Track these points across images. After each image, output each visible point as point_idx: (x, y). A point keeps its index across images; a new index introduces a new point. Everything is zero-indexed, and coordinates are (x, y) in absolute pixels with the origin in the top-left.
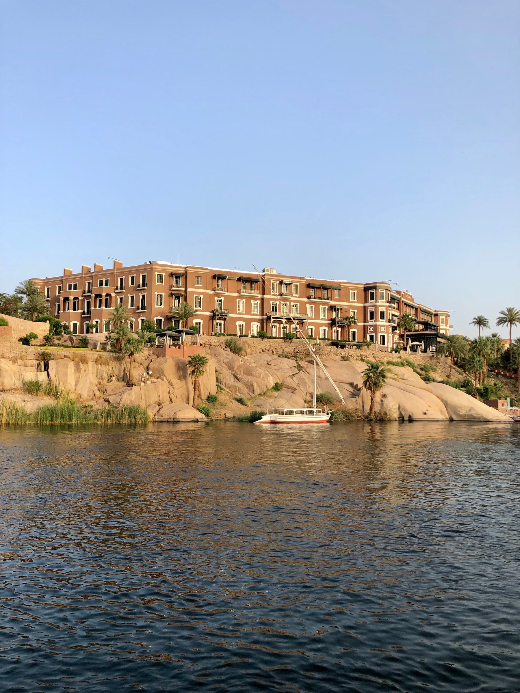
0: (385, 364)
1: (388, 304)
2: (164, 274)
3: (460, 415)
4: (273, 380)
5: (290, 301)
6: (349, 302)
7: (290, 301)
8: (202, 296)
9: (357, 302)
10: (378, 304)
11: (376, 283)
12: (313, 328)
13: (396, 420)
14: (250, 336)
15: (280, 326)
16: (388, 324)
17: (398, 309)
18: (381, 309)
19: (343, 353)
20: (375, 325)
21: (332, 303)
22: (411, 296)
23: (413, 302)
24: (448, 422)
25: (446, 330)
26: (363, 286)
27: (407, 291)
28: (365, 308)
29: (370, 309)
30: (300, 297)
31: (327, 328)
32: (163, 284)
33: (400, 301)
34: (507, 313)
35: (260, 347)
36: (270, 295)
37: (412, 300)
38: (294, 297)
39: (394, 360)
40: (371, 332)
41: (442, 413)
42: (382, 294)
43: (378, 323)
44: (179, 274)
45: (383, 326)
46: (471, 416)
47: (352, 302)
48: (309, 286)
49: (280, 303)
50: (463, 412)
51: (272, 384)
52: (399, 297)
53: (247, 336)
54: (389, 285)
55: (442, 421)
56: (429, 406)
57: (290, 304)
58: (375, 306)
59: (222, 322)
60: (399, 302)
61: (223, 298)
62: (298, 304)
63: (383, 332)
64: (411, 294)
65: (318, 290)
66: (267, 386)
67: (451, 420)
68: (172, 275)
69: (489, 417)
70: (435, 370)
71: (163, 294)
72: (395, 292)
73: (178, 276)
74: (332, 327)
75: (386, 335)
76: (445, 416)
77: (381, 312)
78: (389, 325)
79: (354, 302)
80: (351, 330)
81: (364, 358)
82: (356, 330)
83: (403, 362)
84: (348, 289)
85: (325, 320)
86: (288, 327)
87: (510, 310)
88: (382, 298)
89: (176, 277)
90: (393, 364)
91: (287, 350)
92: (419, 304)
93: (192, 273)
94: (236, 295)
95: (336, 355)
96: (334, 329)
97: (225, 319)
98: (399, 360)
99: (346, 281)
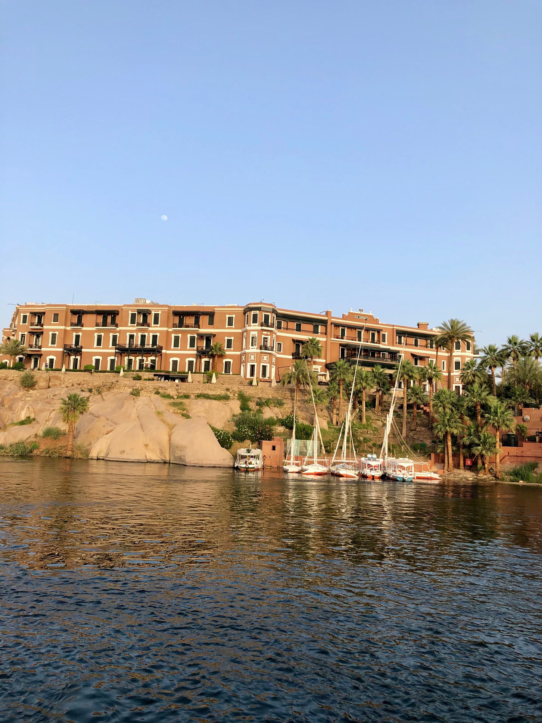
0: (192, 396)
1: (260, 328)
2: (28, 314)
3: (175, 457)
4: (25, 414)
5: (149, 332)
6: (225, 328)
7: (149, 332)
8: (57, 333)
9: (235, 328)
10: (248, 328)
11: (249, 304)
12: (178, 359)
13: (92, 459)
14: (64, 370)
15: (135, 359)
16: (259, 351)
17: (326, 334)
18: (252, 333)
19: (138, 385)
20: (245, 353)
21: (202, 331)
22: (372, 317)
23: (378, 324)
24: (168, 464)
25: (462, 357)
26: (243, 309)
27: (361, 310)
28: (243, 333)
29: (245, 334)
30: (160, 327)
31: (194, 360)
32: (27, 324)
33: (327, 323)
34: (450, 328)
35: (71, 381)
36: (128, 326)
37: (376, 321)
38: (154, 327)
39: (211, 393)
40: (252, 361)
41: (162, 452)
42: (255, 316)
43: (247, 351)
44: (40, 313)
45: (253, 353)
46: (180, 458)
47: (228, 328)
48: (176, 313)
49: (137, 334)
50: (178, 453)
51: (23, 417)
52: (326, 318)
53: (61, 370)
54: (271, 305)
55: (132, 462)
56: (146, 446)
57: (149, 334)
58: (246, 331)
59: (79, 358)
60: (324, 323)
61: (80, 334)
62: (158, 334)
63: (252, 361)
64: (371, 314)
65: (188, 318)
66: (12, 420)
67: (170, 463)
68: (34, 314)
69: (190, 459)
70: (280, 404)
71: (26, 333)
72: (324, 314)
73: (40, 315)
74: (201, 358)
75: (255, 364)
76: (165, 458)
77: (253, 338)
78: (262, 353)
79: (232, 328)
80: (224, 361)
81: (160, 391)
82: (231, 361)
83: (231, 395)
84: (224, 314)
85: (194, 350)
86: (133, 360)
87: (454, 324)
88: (255, 321)
89: (39, 317)
90: (207, 397)
91: (96, 383)
92: (393, 326)
93: (50, 311)
94: (94, 328)
95: (129, 387)
96: (204, 360)
97: (81, 355)
98: (223, 393)
99: (236, 305)
